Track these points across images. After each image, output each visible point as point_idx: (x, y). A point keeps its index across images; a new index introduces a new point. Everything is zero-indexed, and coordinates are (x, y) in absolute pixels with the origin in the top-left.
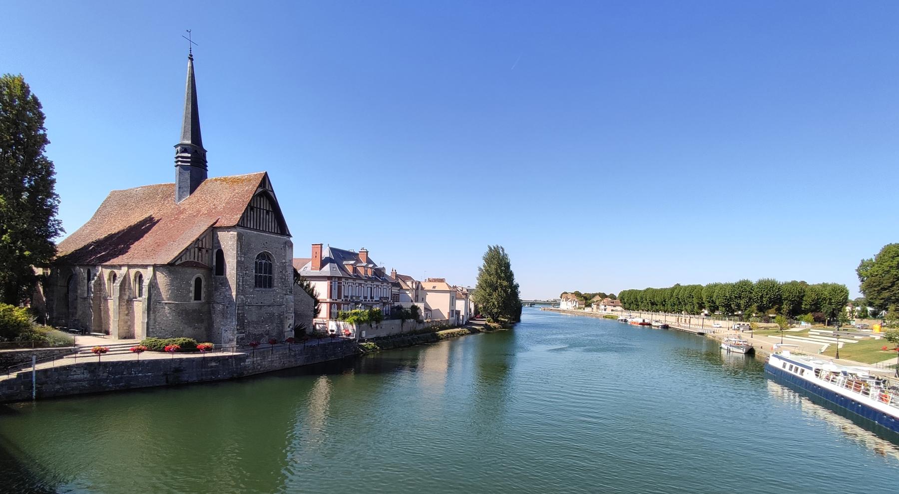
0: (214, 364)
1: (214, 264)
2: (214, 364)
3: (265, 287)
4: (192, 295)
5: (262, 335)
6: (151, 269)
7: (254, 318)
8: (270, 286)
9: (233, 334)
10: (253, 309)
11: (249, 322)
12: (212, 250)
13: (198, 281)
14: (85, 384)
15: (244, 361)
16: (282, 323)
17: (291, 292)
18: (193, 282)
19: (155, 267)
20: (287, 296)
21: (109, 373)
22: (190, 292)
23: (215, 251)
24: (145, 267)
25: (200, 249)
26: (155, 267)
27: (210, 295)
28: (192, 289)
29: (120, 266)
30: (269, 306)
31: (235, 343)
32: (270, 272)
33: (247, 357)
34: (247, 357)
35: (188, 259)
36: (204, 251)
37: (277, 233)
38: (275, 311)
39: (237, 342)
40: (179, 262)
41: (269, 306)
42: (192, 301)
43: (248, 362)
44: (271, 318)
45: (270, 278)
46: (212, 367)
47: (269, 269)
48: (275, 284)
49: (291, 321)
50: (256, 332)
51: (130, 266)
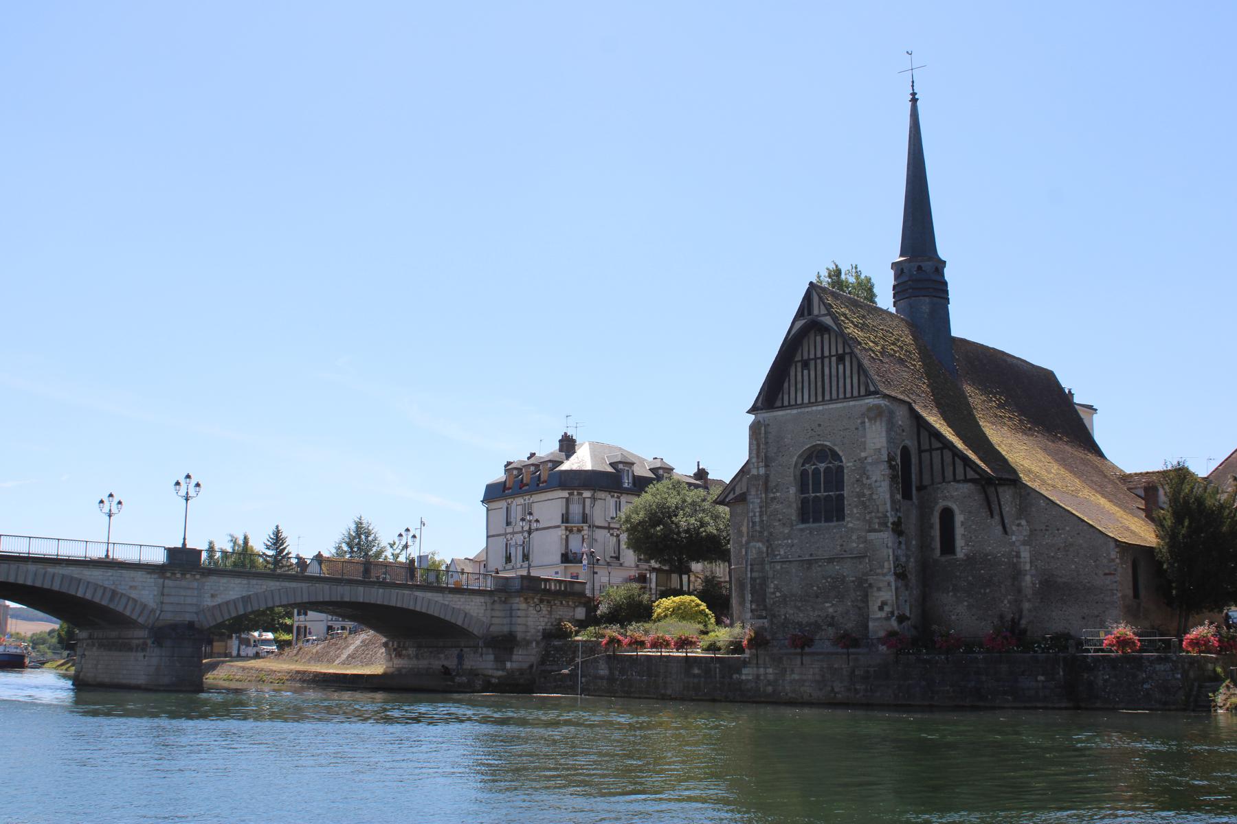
0: (696, 671)
3: (828, 520)
5: (817, 626)
8: (840, 516)
15: (739, 671)
16: (865, 598)
17: (885, 524)
20: (872, 536)
30: (830, 560)
33: (745, 663)
34: (745, 663)
38: (847, 570)
41: (830, 560)
43: (747, 674)
47: (835, 478)
49: (887, 595)
50: (801, 617)
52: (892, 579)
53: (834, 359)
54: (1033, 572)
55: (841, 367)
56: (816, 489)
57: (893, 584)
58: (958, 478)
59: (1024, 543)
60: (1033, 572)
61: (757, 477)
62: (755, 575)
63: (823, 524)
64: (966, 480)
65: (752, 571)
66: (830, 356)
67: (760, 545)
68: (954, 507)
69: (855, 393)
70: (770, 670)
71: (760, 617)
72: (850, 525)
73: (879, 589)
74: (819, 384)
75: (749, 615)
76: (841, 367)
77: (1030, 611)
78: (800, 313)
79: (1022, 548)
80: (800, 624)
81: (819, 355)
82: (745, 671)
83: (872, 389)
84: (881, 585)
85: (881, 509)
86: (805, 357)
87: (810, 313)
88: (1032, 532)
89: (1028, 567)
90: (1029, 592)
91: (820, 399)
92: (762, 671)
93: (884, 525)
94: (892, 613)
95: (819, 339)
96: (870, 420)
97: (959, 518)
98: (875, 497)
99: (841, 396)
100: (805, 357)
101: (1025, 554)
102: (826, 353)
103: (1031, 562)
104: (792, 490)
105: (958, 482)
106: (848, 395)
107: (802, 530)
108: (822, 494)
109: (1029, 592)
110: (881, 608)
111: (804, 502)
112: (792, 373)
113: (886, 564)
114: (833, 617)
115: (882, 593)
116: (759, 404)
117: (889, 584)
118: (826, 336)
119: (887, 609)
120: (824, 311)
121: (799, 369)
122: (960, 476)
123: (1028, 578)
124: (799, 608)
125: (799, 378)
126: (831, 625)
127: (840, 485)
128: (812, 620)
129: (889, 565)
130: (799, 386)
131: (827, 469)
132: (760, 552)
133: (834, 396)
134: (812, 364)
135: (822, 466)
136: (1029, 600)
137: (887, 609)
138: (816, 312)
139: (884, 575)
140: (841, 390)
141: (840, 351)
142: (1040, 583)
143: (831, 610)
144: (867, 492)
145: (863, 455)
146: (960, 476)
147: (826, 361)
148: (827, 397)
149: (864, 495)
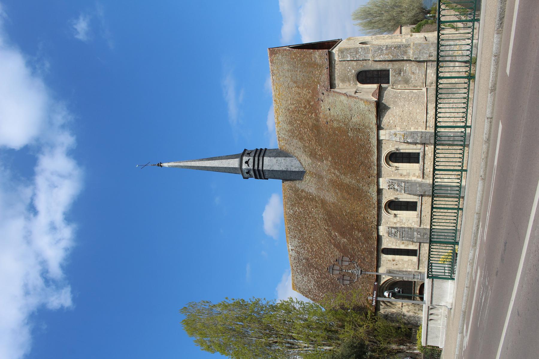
19: (379, 128)
23: (360, 85)
26: (379, 128)
29: (379, 192)
48: (399, 40)
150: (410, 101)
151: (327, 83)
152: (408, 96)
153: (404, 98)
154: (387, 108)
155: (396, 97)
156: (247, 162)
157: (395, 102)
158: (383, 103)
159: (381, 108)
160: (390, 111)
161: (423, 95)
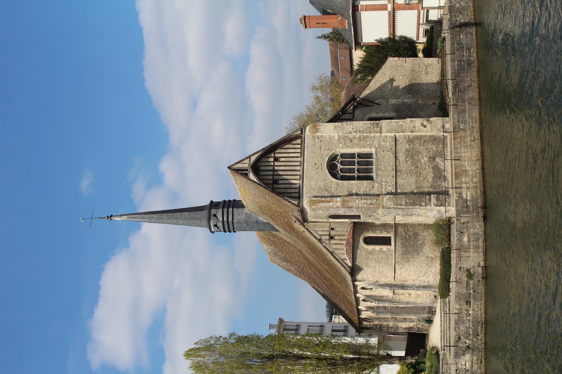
0: (465, 239)
1: (347, 220)
2: (465, 239)
3: (371, 163)
4: (385, 248)
6: (356, 283)
7: (412, 180)
8: (369, 156)
9: (431, 210)
10: (400, 181)
11: (417, 187)
12: (330, 223)
13: (369, 241)
14: (475, 358)
16: (419, 138)
18: (370, 247)
19: (354, 280)
20: (384, 130)
21: (467, 338)
22: (381, 250)
23: (331, 220)
24: (355, 287)
25: (332, 238)
26: (354, 280)
27: (385, 226)
28: (377, 248)
29: (356, 297)
31: (443, 208)
32: (354, 154)
33: (460, 195)
34: (460, 195)
35: (344, 252)
36: (333, 233)
37: (302, 144)
38: (403, 147)
39: (441, 205)
40: (350, 264)
42: (392, 247)
44: (412, 155)
45: (360, 155)
46: (469, 241)
49: (418, 122)
51: (356, 292)
52: (408, 120)
53: (276, 164)
54: (403, 97)
55: (282, 159)
56: (352, 171)
57: (412, 119)
58: (352, 118)
59: (387, 102)
60: (403, 97)
61: (344, 201)
62: (403, 203)
63: (374, 167)
64: (353, 113)
65: (400, 205)
66: (274, 166)
67: (385, 199)
68: (368, 117)
69: (299, 150)
70: (463, 180)
71: (430, 200)
72: (376, 146)
73: (414, 127)
74: (289, 173)
75: (428, 207)
76: (282, 159)
77: (423, 100)
78: (246, 175)
79: (390, 103)
80: (434, 178)
81: (271, 173)
82: (464, 196)
83: (299, 132)
84: (412, 126)
85: (369, 126)
86: (271, 182)
87: (247, 170)
88: (382, 97)
89: (400, 100)
90: (413, 100)
91: (298, 173)
92: (464, 185)
93: (378, 124)
94: (428, 120)
95: (262, 173)
96: (317, 131)
97: (374, 115)
98: (362, 129)
99: (299, 159)
100: (271, 182)
101: (393, 101)
102: (271, 168)
103: (398, 99)
104: (353, 182)
105: (354, 116)
106: (299, 155)
107: (377, 175)
108: (356, 167)
109: (413, 100)
110: (425, 126)
111: (360, 178)
112: (280, 191)
113: (400, 123)
114: (430, 158)
115: (417, 126)
116: (296, 203)
117: (412, 121)
118: (262, 168)
119: (425, 123)
120: (247, 161)
121: (278, 186)
122: (350, 116)
123: (406, 100)
124: (425, 178)
125: (283, 186)
126: (434, 159)
127: (352, 156)
128: (431, 170)
129: (400, 122)
130: (288, 186)
131: (342, 163)
132: (390, 199)
133: (298, 164)
134: (276, 177)
135: (339, 166)
136: (418, 100)
137: (425, 123)
138: (247, 165)
139: (406, 123)
140: (295, 159)
141: (272, 159)
142: (409, 94)
143: (426, 159)
144: (358, 136)
145: (336, 138)
146: (350, 116)
147: (276, 168)
148: (298, 168)
149: (360, 137)
150: (380, 262)
151: (300, 218)
152: (378, 257)
153: (375, 260)
154: (360, 269)
155: (368, 259)
156: (215, 226)
157: (367, 264)
158: (356, 265)
159: (354, 271)
160: (363, 271)
161: (392, 255)
